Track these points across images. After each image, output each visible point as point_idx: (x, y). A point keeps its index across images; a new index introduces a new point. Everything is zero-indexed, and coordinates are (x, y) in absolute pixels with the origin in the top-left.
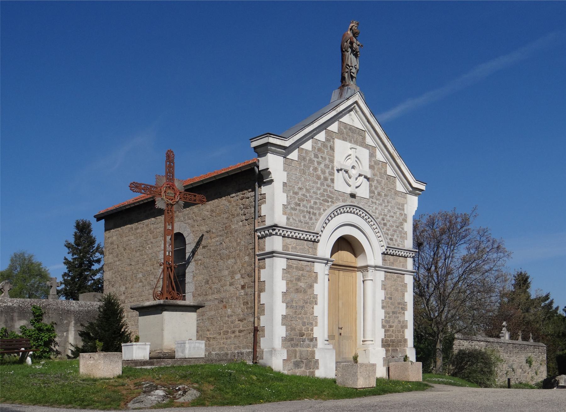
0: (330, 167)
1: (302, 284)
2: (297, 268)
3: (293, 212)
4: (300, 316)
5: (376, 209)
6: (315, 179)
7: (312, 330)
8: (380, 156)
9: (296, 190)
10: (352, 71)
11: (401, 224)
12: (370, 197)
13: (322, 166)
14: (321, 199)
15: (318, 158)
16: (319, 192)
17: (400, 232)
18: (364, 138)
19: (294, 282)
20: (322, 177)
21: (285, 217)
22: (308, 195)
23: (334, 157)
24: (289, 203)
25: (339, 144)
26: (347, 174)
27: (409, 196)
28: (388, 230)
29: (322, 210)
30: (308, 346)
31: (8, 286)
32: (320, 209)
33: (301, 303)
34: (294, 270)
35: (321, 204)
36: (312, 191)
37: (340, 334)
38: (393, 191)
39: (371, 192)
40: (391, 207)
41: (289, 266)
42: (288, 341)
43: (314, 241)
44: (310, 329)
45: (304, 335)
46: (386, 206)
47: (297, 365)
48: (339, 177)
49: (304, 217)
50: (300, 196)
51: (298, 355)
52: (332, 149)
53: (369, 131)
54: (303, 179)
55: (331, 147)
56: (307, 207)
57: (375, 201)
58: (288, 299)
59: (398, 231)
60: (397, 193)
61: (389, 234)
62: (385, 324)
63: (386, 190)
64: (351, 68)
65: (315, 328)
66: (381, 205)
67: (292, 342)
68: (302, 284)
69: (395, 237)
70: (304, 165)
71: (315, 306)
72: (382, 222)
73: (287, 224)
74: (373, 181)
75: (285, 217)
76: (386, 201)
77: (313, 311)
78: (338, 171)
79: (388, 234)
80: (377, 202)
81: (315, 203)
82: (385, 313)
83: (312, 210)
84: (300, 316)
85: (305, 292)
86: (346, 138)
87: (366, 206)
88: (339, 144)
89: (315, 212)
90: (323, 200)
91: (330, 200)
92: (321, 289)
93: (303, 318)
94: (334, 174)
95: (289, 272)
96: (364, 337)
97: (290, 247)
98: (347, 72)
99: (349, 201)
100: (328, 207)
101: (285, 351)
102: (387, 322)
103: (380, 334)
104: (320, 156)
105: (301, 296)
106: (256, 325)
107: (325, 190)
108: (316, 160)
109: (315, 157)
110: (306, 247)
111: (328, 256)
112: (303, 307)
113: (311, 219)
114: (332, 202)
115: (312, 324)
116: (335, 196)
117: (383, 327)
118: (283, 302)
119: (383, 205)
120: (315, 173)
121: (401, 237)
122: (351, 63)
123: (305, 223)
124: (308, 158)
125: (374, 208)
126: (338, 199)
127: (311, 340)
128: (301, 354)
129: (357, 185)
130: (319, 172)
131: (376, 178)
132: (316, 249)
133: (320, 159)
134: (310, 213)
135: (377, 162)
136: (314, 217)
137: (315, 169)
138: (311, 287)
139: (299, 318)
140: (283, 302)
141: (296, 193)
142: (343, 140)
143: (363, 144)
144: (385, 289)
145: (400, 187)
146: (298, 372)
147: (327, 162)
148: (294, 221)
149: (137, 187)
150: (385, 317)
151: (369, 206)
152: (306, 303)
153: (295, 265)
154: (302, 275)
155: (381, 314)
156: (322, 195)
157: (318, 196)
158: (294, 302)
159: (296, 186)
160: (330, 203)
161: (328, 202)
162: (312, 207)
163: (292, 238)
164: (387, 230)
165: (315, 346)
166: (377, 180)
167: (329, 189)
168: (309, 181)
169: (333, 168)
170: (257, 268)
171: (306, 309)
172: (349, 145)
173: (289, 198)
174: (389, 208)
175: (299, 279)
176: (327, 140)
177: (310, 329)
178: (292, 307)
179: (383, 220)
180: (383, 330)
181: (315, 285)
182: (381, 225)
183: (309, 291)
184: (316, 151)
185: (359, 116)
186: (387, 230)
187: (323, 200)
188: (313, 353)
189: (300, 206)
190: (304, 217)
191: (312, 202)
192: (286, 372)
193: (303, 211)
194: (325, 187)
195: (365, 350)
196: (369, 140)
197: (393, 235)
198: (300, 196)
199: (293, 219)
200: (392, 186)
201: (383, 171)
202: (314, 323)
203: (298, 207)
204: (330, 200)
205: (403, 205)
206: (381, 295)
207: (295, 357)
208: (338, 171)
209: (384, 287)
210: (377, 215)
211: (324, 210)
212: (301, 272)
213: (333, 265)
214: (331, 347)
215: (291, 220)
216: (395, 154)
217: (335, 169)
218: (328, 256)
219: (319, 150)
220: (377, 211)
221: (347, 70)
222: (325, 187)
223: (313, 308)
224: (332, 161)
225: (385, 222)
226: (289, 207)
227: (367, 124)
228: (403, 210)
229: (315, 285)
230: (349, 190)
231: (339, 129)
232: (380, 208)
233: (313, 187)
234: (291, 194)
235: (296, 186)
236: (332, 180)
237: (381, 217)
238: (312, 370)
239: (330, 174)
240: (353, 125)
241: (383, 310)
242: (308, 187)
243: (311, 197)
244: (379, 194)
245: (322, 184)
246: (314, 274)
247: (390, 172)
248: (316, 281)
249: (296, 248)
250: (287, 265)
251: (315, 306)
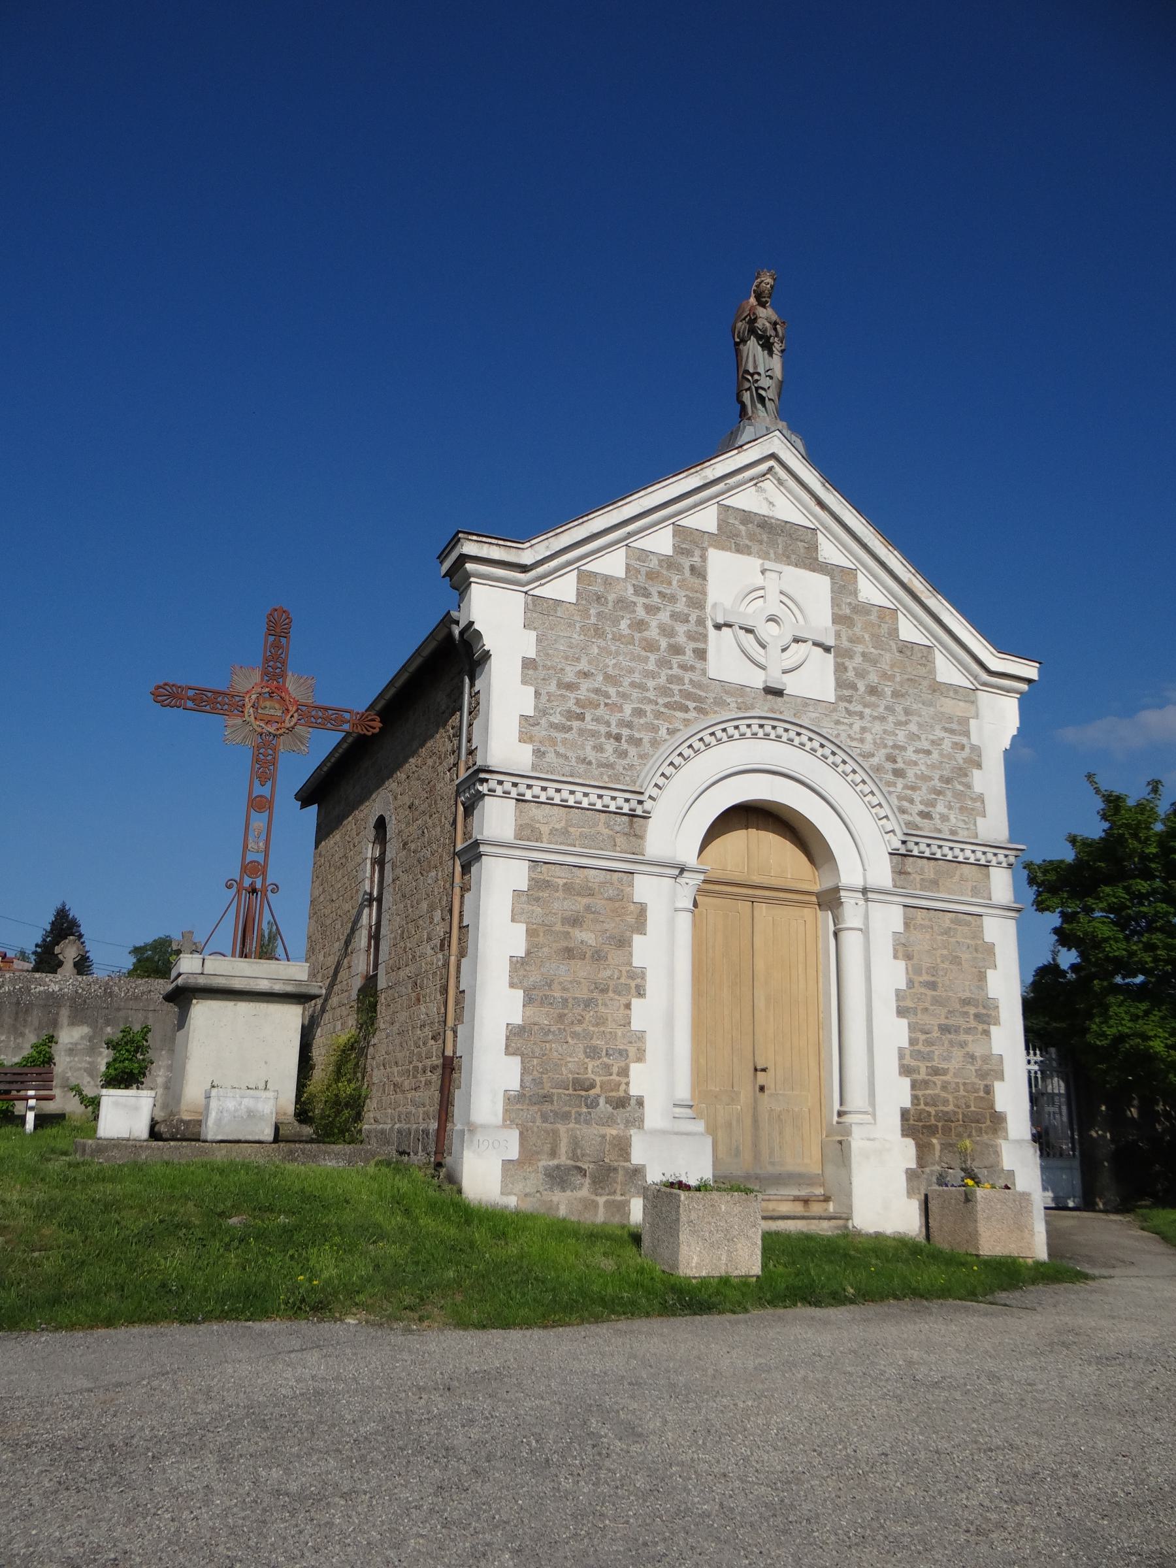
0: (693, 618)
1: (586, 936)
2: (568, 888)
3: (560, 736)
4: (578, 1029)
5: (863, 729)
6: (638, 650)
7: (624, 1072)
8: (869, 591)
9: (570, 676)
10: (760, 384)
11: (962, 773)
12: (840, 698)
13: (664, 616)
14: (661, 701)
15: (647, 595)
16: (651, 684)
17: (959, 795)
18: (813, 547)
19: (558, 927)
20: (664, 644)
21: (529, 748)
22: (612, 691)
23: (704, 593)
24: (542, 712)
25: (719, 561)
26: (751, 636)
27: (983, 697)
28: (913, 788)
29: (663, 732)
30: (610, 1121)
31: (75, 949)
32: (655, 729)
33: (582, 993)
34: (560, 894)
35: (658, 715)
36: (626, 682)
37: (762, 1089)
38: (925, 683)
39: (840, 684)
40: (919, 725)
41: (537, 884)
42: (535, 1104)
43: (632, 816)
44: (615, 1070)
45: (592, 1086)
46: (899, 724)
47: (559, 1178)
48: (721, 646)
49: (599, 748)
50: (583, 692)
51: (563, 1148)
52: (699, 573)
53: (826, 528)
54: (596, 651)
55: (693, 569)
56: (608, 724)
57: (859, 708)
58: (534, 977)
59: (949, 794)
60: (937, 688)
61: (917, 799)
62: (913, 1063)
63: (898, 679)
64: (756, 377)
65: (635, 1068)
66: (882, 719)
67: (547, 1107)
68: (586, 936)
69: (940, 808)
70: (599, 614)
71: (636, 1002)
72: (889, 766)
73: (534, 767)
74: (851, 657)
75: (529, 748)
76: (899, 709)
77: (629, 1017)
78: (718, 627)
79: (912, 801)
80: (867, 711)
81: (639, 712)
82: (912, 1028)
83: (625, 732)
84: (578, 1029)
85: (598, 957)
86: (749, 547)
87: (825, 724)
88: (719, 561)
89: (637, 735)
90: (666, 705)
91: (691, 705)
92: (665, 951)
93: (589, 1036)
94: (705, 636)
95: (537, 899)
96: (841, 1105)
97: (545, 830)
98: (749, 389)
99: (763, 707)
100: (687, 723)
101: (514, 1136)
102: (918, 1055)
103: (897, 1094)
104: (654, 591)
105: (582, 970)
106: (449, 1053)
107: (671, 679)
108: (641, 600)
109: (636, 593)
110: (606, 831)
111: (689, 856)
112: (588, 1003)
113: (623, 754)
114: (699, 710)
115: (623, 1054)
116: (712, 695)
117: (905, 1070)
118: (512, 985)
119: (891, 719)
120: (637, 636)
121: (961, 809)
122: (755, 367)
123: (601, 765)
124: (611, 597)
125: (856, 727)
126: (720, 703)
127: (622, 1103)
128: (575, 1143)
129: (787, 665)
130: (653, 633)
131: (859, 649)
132: (640, 837)
133: (656, 599)
134: (618, 738)
135: (863, 609)
136: (633, 751)
137: (640, 625)
138: (623, 943)
139: (575, 1035)
140: (512, 985)
141: (570, 687)
142: (739, 550)
143: (811, 561)
144: (908, 957)
145: (947, 671)
146: (565, 1204)
147: (681, 606)
148: (561, 761)
149: (172, 695)
150: (913, 1042)
151: (838, 723)
152: (604, 991)
153: (561, 882)
154: (588, 908)
155: (894, 1033)
156: (664, 691)
157: (651, 695)
158: (555, 986)
159: (568, 668)
160: (692, 715)
161: (686, 709)
162: (622, 723)
163: (550, 803)
164: (906, 787)
165: (638, 1122)
166: (864, 655)
167: (687, 676)
168: (617, 653)
169: (701, 622)
170: (457, 890)
171: (602, 1009)
172: (755, 563)
173: (544, 698)
174: (913, 727)
175: (575, 921)
176: (679, 550)
177: (615, 1070)
178: (545, 1001)
179: (892, 759)
180: (907, 1082)
181: (637, 939)
182: (884, 772)
183: (615, 957)
184: (642, 578)
185: (790, 492)
186: (906, 787)
187: (666, 705)
188: (623, 1147)
189: (583, 719)
190: (599, 748)
191: (628, 709)
192: (512, 1201)
193: (594, 734)
194: (676, 671)
195: (840, 1142)
196: (829, 551)
197: (932, 804)
198: (583, 692)
199: (557, 754)
200: (922, 671)
201: (885, 628)
202: (632, 1051)
203: (576, 724)
204: (691, 705)
205: (964, 721)
206: (892, 976)
207: (553, 1153)
208: (718, 627)
209: (903, 950)
210: (868, 747)
211: (671, 732)
212: (585, 901)
213: (705, 881)
214: (699, 1126)
215: (551, 757)
216: (918, 584)
217: (709, 624)
218: (689, 856)
219: (652, 576)
220: (869, 737)
221: (747, 385)
222: (676, 671)
223: (628, 1006)
224: (698, 603)
225: (900, 765)
226: (543, 721)
227: (817, 509)
228: (967, 734)
229: (637, 939)
230: (757, 680)
231: (722, 523)
232: (878, 727)
233: (631, 671)
234: (553, 687)
235: (568, 668)
236: (701, 654)
237: (884, 751)
238: (619, 1198)
239: (691, 637)
240: (771, 514)
241: (904, 1022)
242: (610, 671)
243: (624, 696)
244: (873, 690)
245: (663, 663)
246: (632, 907)
247: (908, 631)
248: (640, 926)
249: (565, 832)
250: (531, 879)
251: (636, 1002)
